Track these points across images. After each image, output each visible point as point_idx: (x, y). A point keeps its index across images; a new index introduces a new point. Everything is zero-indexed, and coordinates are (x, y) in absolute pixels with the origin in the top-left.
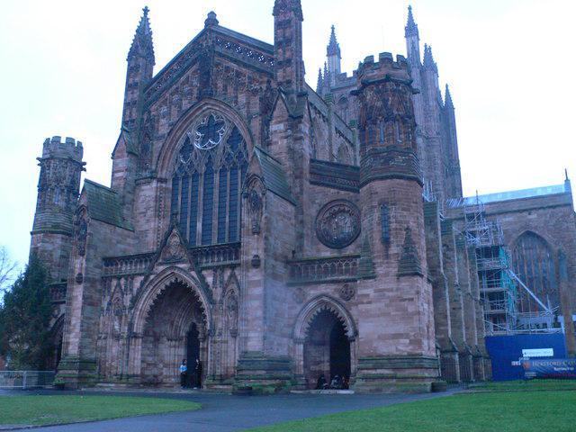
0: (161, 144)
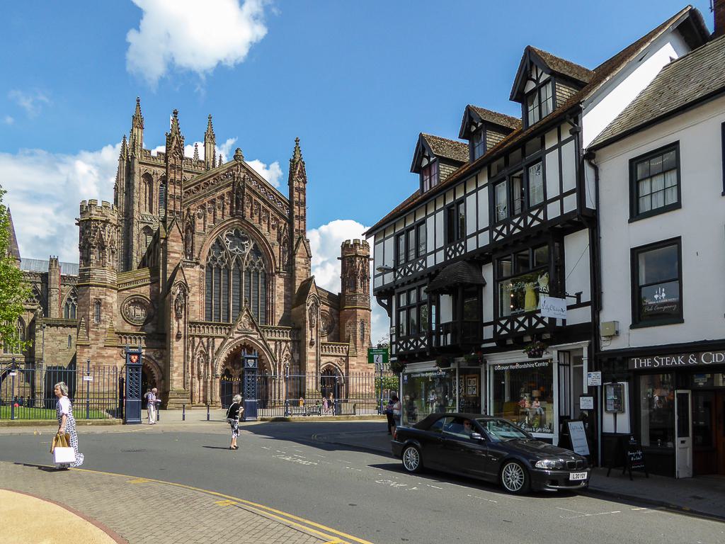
0: (201, 239)
